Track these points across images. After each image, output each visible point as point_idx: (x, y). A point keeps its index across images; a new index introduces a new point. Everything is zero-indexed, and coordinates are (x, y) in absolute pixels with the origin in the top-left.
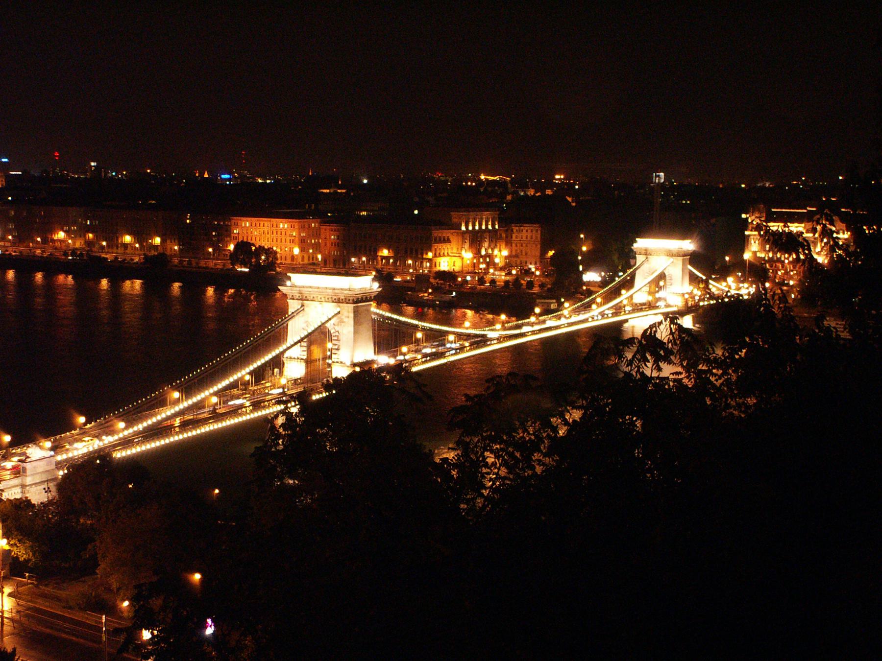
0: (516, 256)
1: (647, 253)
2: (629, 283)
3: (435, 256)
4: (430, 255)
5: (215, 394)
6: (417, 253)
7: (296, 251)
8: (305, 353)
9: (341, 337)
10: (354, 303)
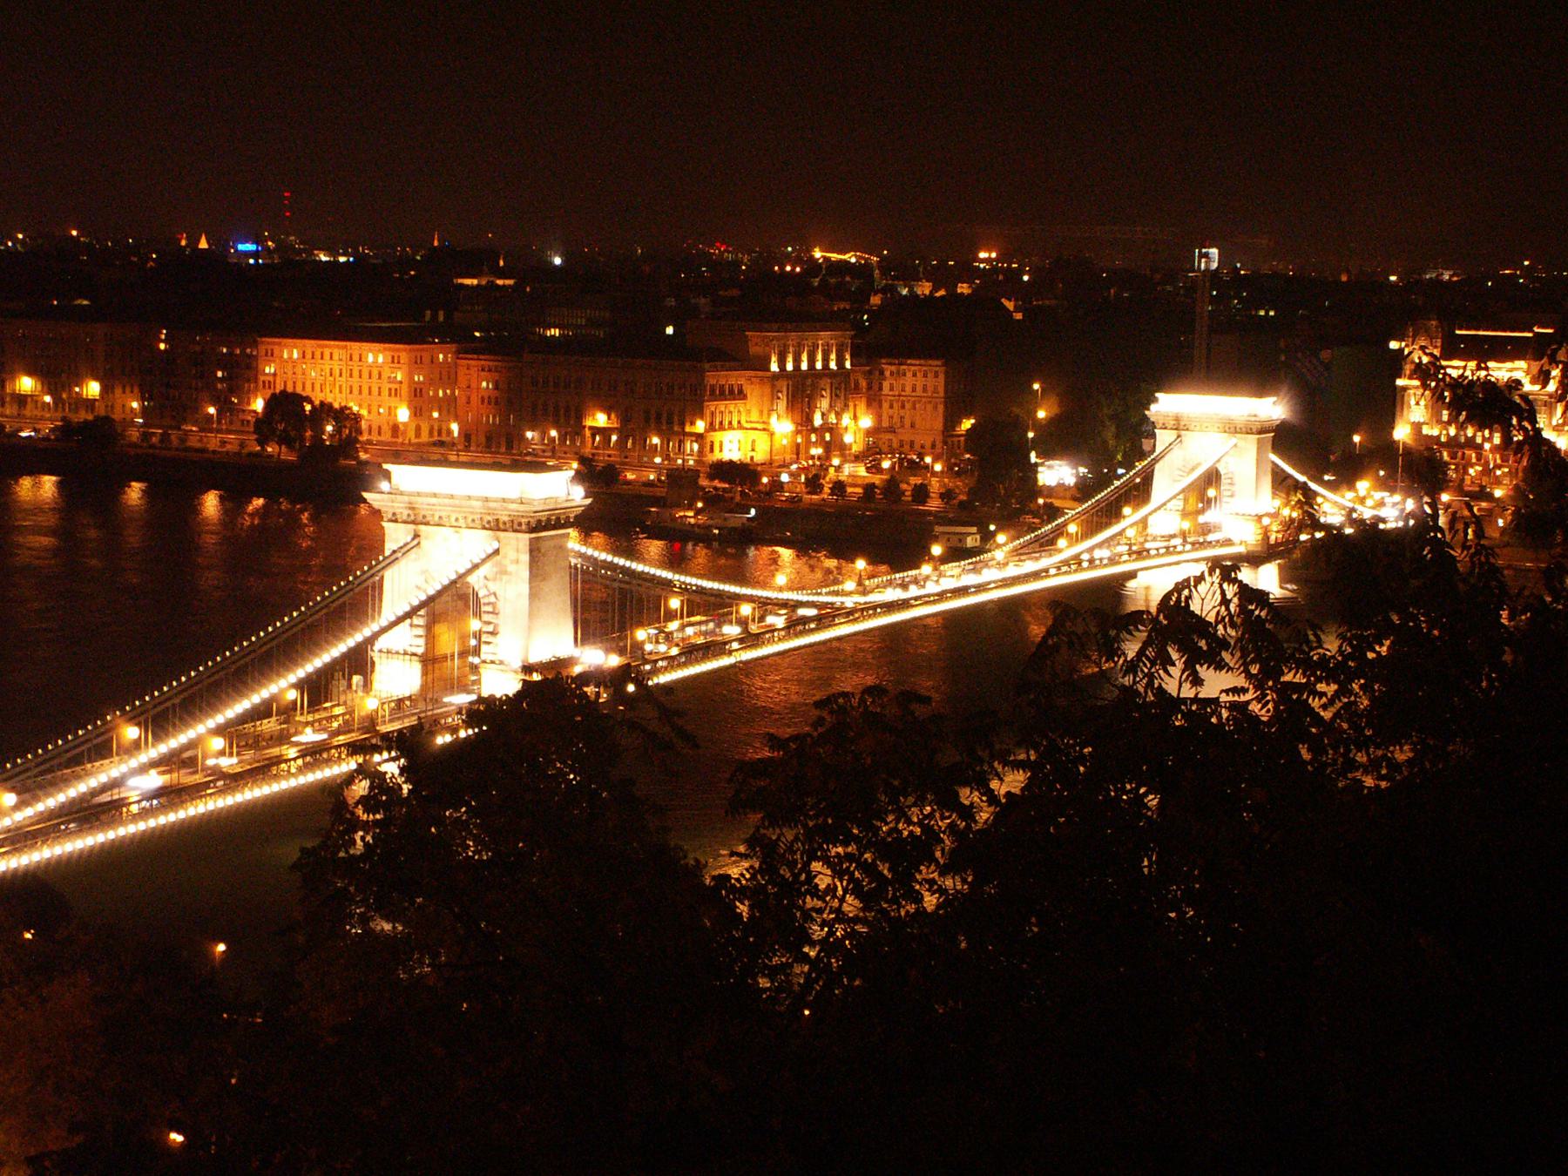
0: (891, 430)
1: (1179, 426)
2: (1140, 492)
3: (711, 428)
4: (700, 426)
5: (219, 731)
6: (670, 422)
7: (403, 414)
8: (422, 642)
9: (500, 605)
10: (532, 530)
